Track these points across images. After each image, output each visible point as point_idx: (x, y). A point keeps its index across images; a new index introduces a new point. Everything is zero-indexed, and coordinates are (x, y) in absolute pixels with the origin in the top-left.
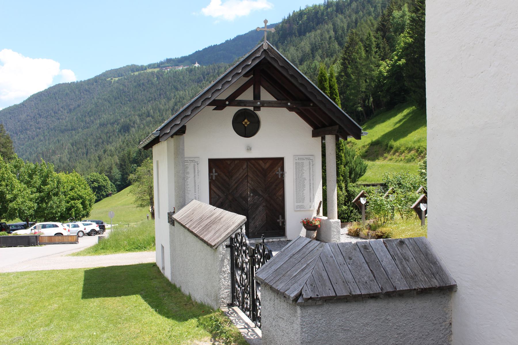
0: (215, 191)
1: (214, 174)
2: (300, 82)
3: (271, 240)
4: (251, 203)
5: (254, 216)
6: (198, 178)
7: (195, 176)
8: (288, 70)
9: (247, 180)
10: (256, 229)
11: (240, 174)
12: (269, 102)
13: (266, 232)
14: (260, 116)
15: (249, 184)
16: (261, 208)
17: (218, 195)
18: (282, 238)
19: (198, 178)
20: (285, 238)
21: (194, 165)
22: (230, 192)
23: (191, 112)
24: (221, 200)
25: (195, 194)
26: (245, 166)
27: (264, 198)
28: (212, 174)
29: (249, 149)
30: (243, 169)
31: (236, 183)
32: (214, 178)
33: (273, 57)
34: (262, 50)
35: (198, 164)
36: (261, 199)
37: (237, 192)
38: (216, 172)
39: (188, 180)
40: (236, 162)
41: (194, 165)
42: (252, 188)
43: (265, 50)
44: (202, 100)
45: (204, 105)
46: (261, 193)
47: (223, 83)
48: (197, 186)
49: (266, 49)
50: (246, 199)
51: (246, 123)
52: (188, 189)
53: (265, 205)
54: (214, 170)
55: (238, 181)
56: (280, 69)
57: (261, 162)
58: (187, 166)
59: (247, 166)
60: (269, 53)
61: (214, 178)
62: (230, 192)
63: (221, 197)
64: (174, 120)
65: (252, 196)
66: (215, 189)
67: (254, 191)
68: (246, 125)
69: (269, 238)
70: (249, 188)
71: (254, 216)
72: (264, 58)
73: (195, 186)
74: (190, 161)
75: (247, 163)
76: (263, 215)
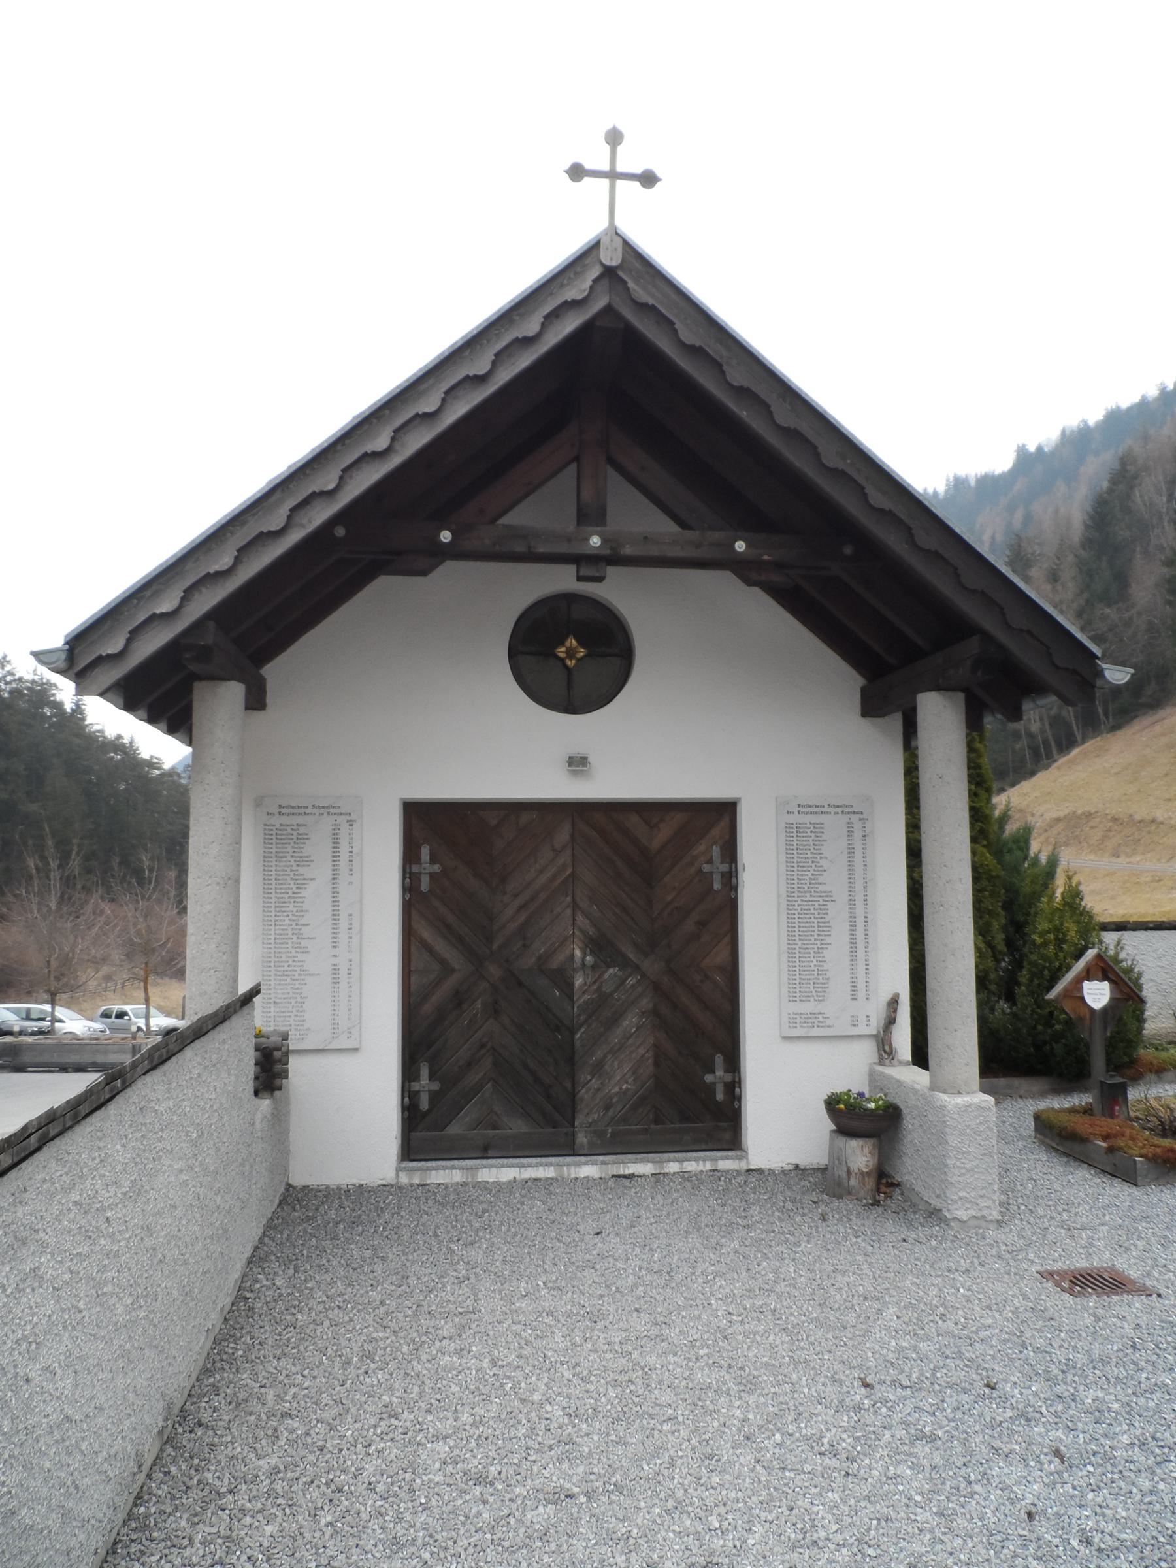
0: (430, 941)
1: (427, 866)
2: (781, 420)
3: (673, 1167)
4: (587, 997)
5: (599, 1054)
6: (351, 883)
7: (335, 877)
8: (725, 368)
9: (569, 899)
10: (610, 1113)
11: (541, 872)
12: (646, 538)
13: (653, 1126)
14: (626, 616)
15: (580, 918)
16: (630, 1022)
17: (442, 961)
18: (722, 1159)
19: (351, 883)
20: (740, 1158)
21: (336, 828)
22: (495, 946)
23: (237, 560)
24: (450, 984)
25: (335, 951)
26: (563, 835)
27: (643, 975)
28: (415, 869)
29: (578, 764)
30: (554, 850)
31: (522, 907)
32: (425, 885)
33: (651, 301)
34: (596, 272)
35: (351, 823)
36: (631, 981)
37: (524, 946)
38: (433, 860)
39: (304, 893)
40: (524, 818)
41: (336, 828)
42: (591, 931)
43: (609, 273)
44: (292, 502)
45: (303, 526)
46: (631, 956)
47: (399, 421)
48: (343, 916)
49: (614, 263)
50: (562, 979)
51: (571, 653)
52: (305, 930)
53: (651, 1006)
54: (425, 852)
55: (532, 899)
56: (684, 363)
57: (634, 819)
58: (302, 830)
59: (572, 836)
60: (631, 284)
61: (425, 885)
62: (495, 946)
63: (453, 970)
64: (148, 593)
65: (592, 967)
66: (427, 934)
67: (602, 948)
68: (571, 663)
69: (666, 1156)
70: (581, 930)
71: (599, 1054)
72: (608, 310)
73: (335, 916)
74: (317, 811)
75: (573, 824)
76: (642, 1051)
